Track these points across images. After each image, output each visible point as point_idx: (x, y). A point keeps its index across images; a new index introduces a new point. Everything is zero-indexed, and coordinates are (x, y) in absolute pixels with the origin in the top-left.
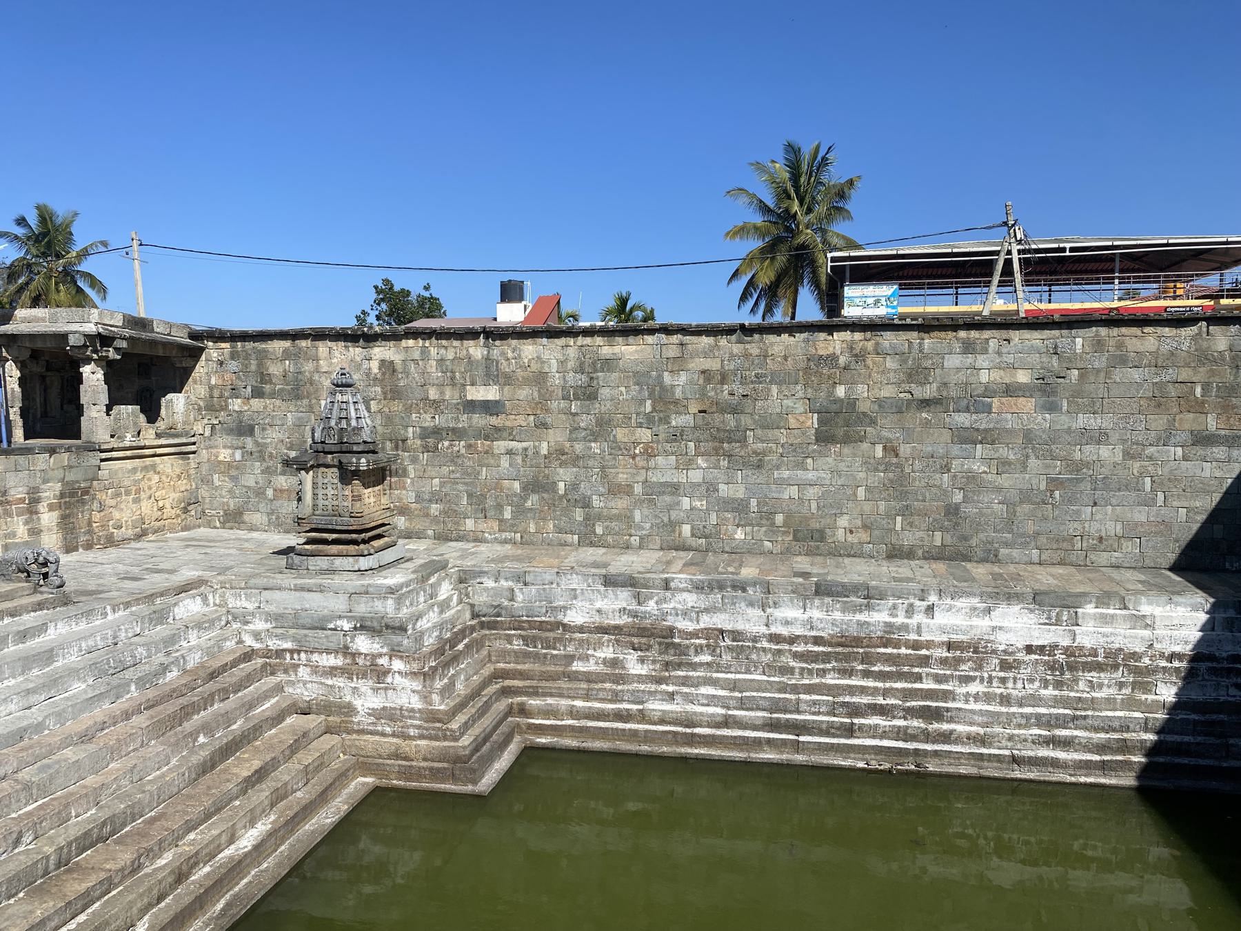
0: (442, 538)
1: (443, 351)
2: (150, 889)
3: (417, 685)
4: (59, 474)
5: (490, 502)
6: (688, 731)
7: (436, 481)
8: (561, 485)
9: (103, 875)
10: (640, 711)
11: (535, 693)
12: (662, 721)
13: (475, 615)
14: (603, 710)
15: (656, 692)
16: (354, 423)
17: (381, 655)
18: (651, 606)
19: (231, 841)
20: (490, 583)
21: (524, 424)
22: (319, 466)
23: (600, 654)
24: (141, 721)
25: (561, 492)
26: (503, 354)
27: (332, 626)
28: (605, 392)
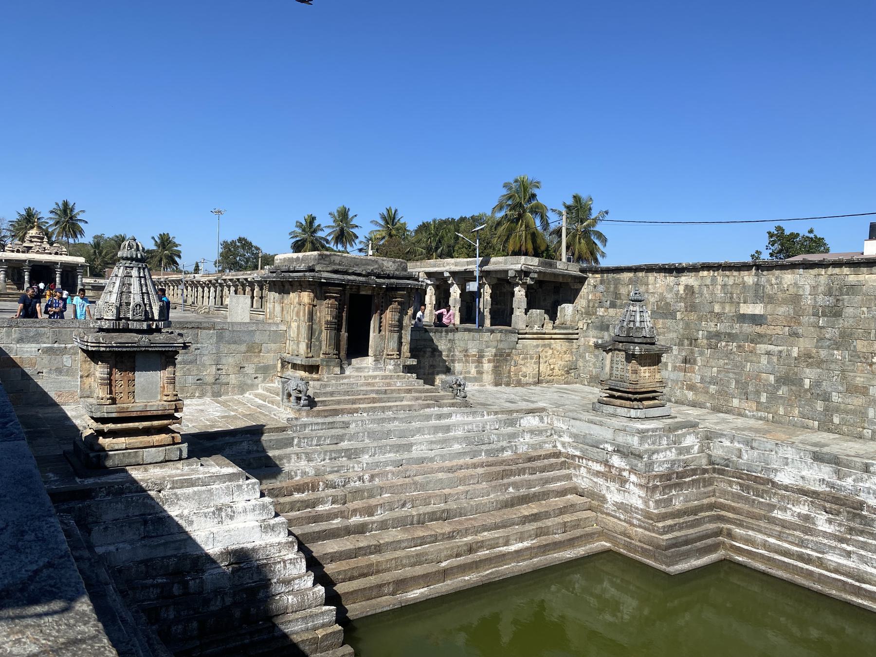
0: (716, 409)
1: (726, 279)
2: (452, 548)
3: (642, 493)
4: (495, 344)
5: (751, 388)
6: (857, 584)
7: (715, 369)
8: (807, 381)
9: (433, 533)
10: (819, 558)
11: (740, 525)
12: (836, 571)
13: (711, 463)
14: (789, 550)
15: (835, 547)
16: (638, 324)
17: (624, 470)
18: (849, 482)
19: (507, 544)
20: (726, 443)
21: (781, 333)
22: (615, 350)
23: (797, 509)
24: (480, 470)
25: (807, 386)
26: (768, 281)
27: (602, 447)
28: (849, 311)
